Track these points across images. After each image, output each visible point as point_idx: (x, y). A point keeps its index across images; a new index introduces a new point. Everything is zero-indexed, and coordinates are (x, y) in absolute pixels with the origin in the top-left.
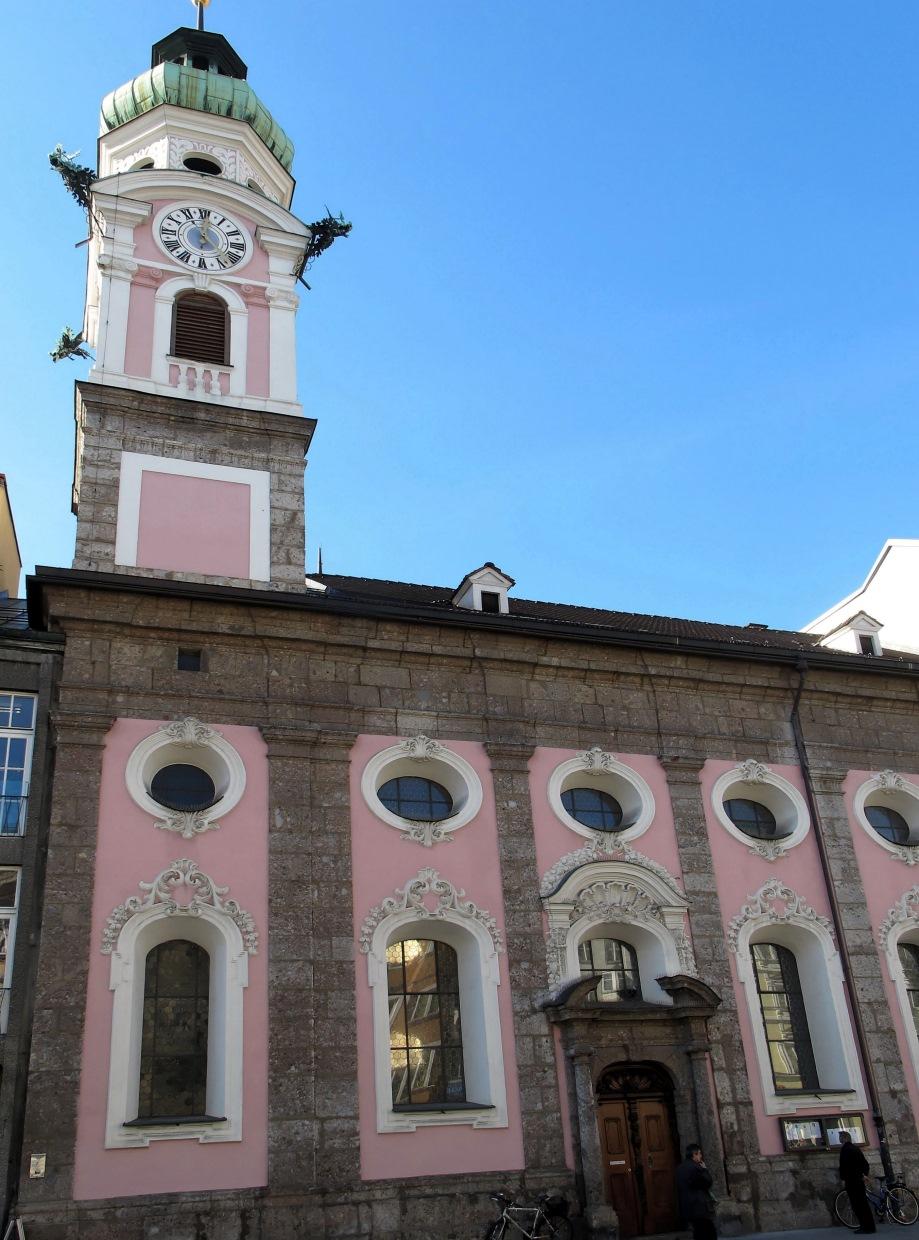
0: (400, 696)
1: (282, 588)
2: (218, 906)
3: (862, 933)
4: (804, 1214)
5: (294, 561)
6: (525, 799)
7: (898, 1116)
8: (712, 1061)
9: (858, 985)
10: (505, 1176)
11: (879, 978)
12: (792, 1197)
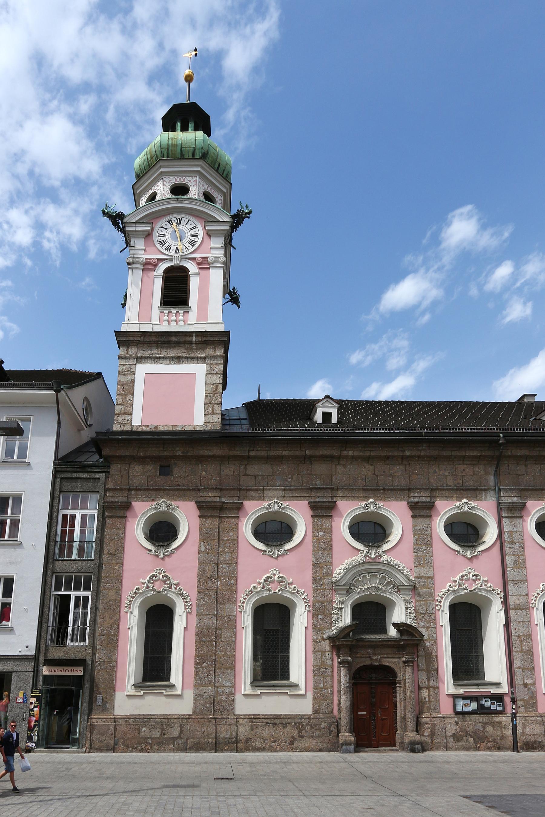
0: (266, 480)
1: (208, 428)
2: (173, 590)
3: (521, 597)
4: (460, 744)
5: (215, 412)
6: (329, 532)
7: (526, 697)
8: (418, 665)
9: (513, 626)
10: (302, 717)
12: (454, 735)
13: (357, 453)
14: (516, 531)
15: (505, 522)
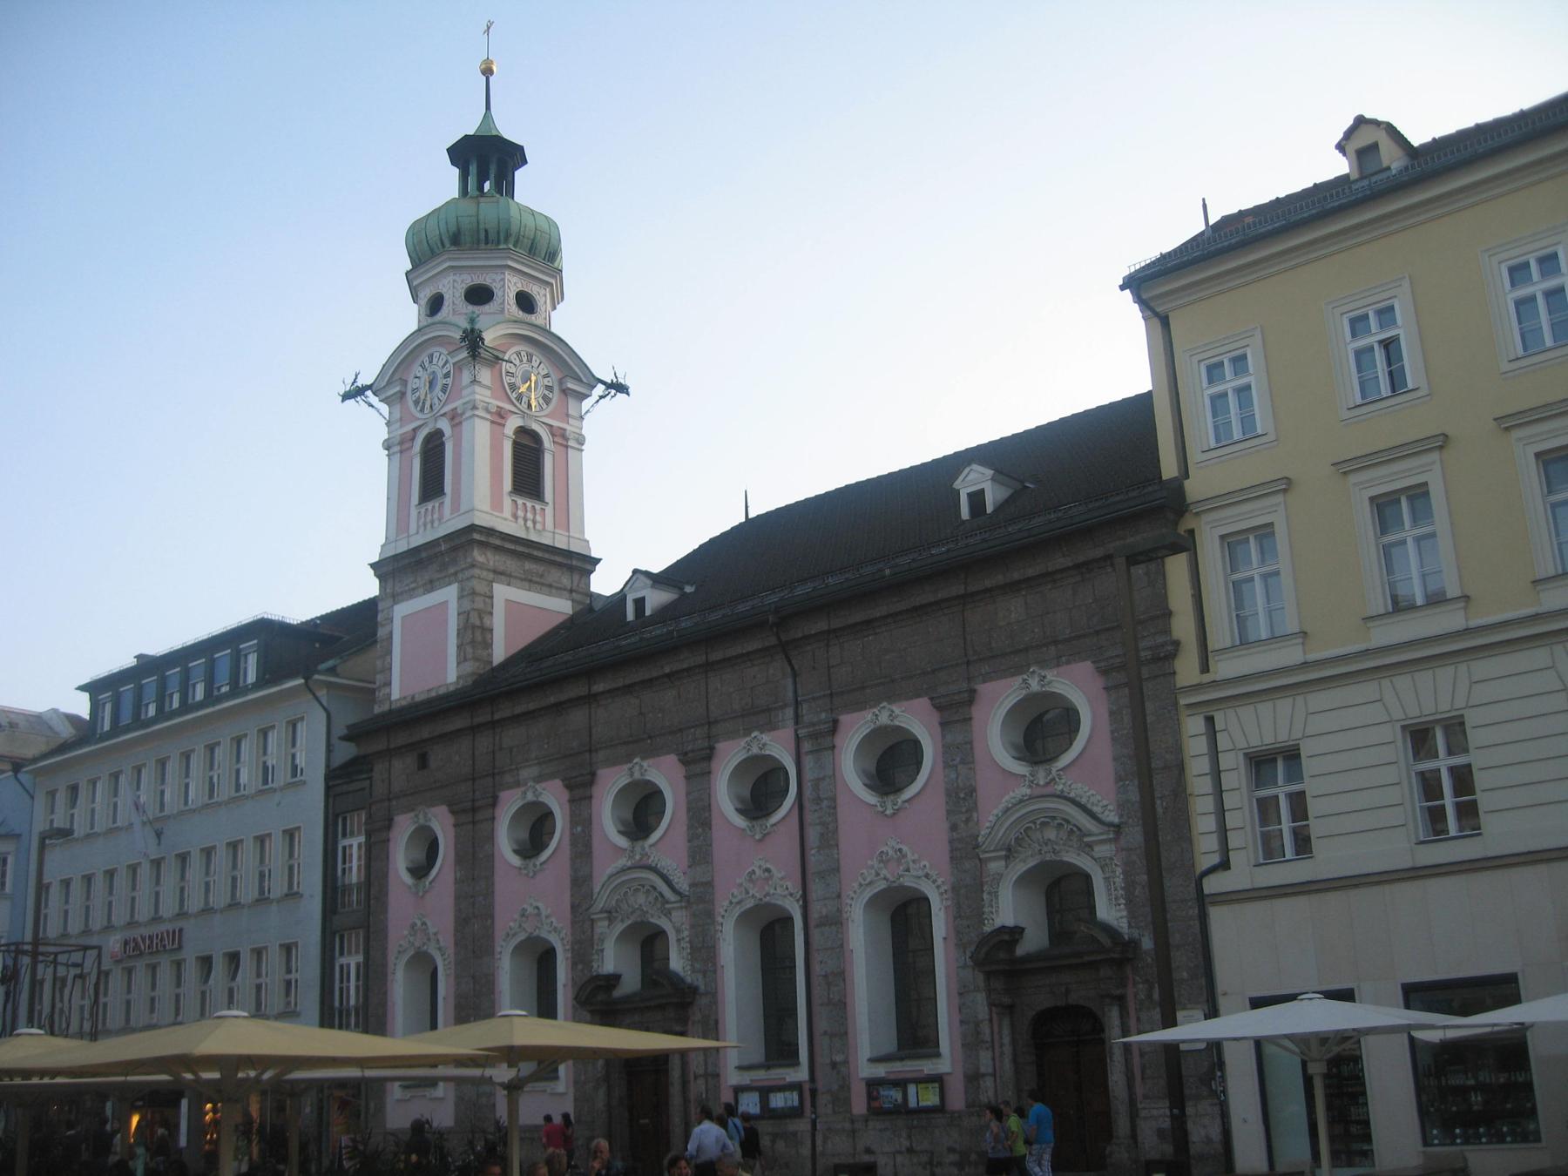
7: (835, 1087)
11: (840, 948)
13: (608, 687)
14: (823, 779)
15: (808, 762)
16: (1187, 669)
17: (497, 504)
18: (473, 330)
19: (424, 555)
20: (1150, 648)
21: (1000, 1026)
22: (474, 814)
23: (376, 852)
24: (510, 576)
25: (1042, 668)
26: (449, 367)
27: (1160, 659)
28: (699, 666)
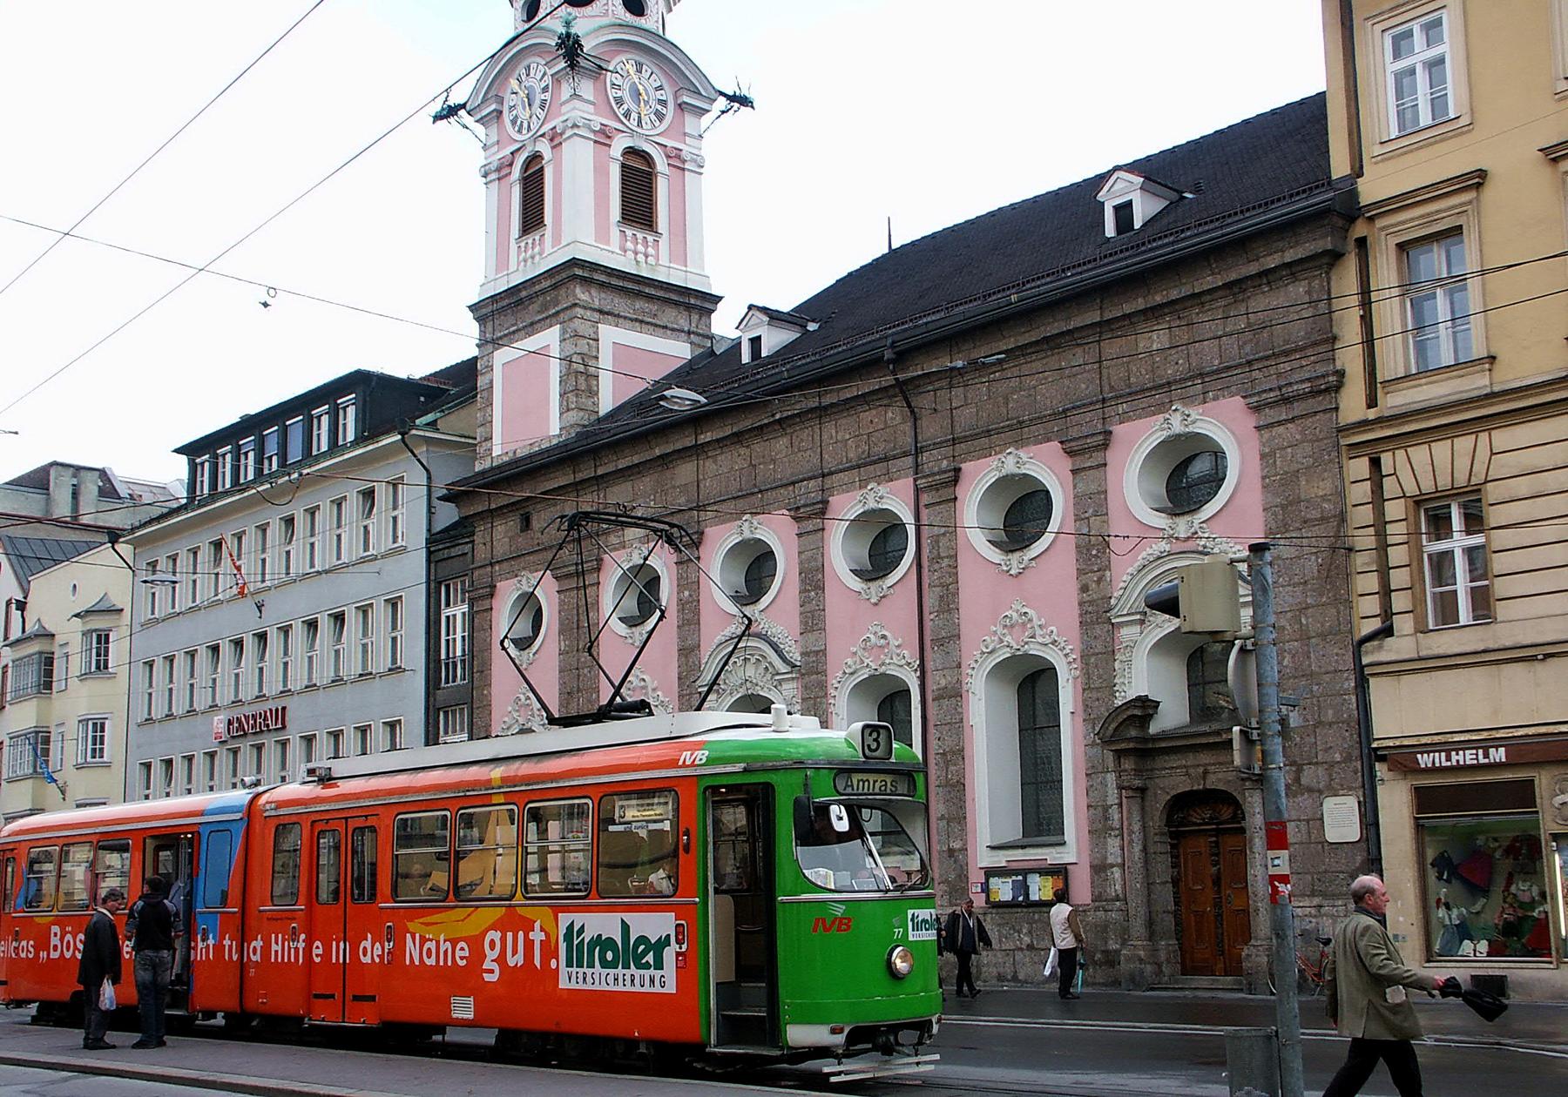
11: (957, 724)
16: (1352, 405)
17: (602, 234)
18: (568, 35)
19: (524, 294)
20: (1309, 380)
21: (1129, 811)
22: (579, 579)
23: (478, 621)
24: (618, 316)
25: (1185, 405)
26: (548, 80)
27: (1320, 392)
28: (812, 410)
